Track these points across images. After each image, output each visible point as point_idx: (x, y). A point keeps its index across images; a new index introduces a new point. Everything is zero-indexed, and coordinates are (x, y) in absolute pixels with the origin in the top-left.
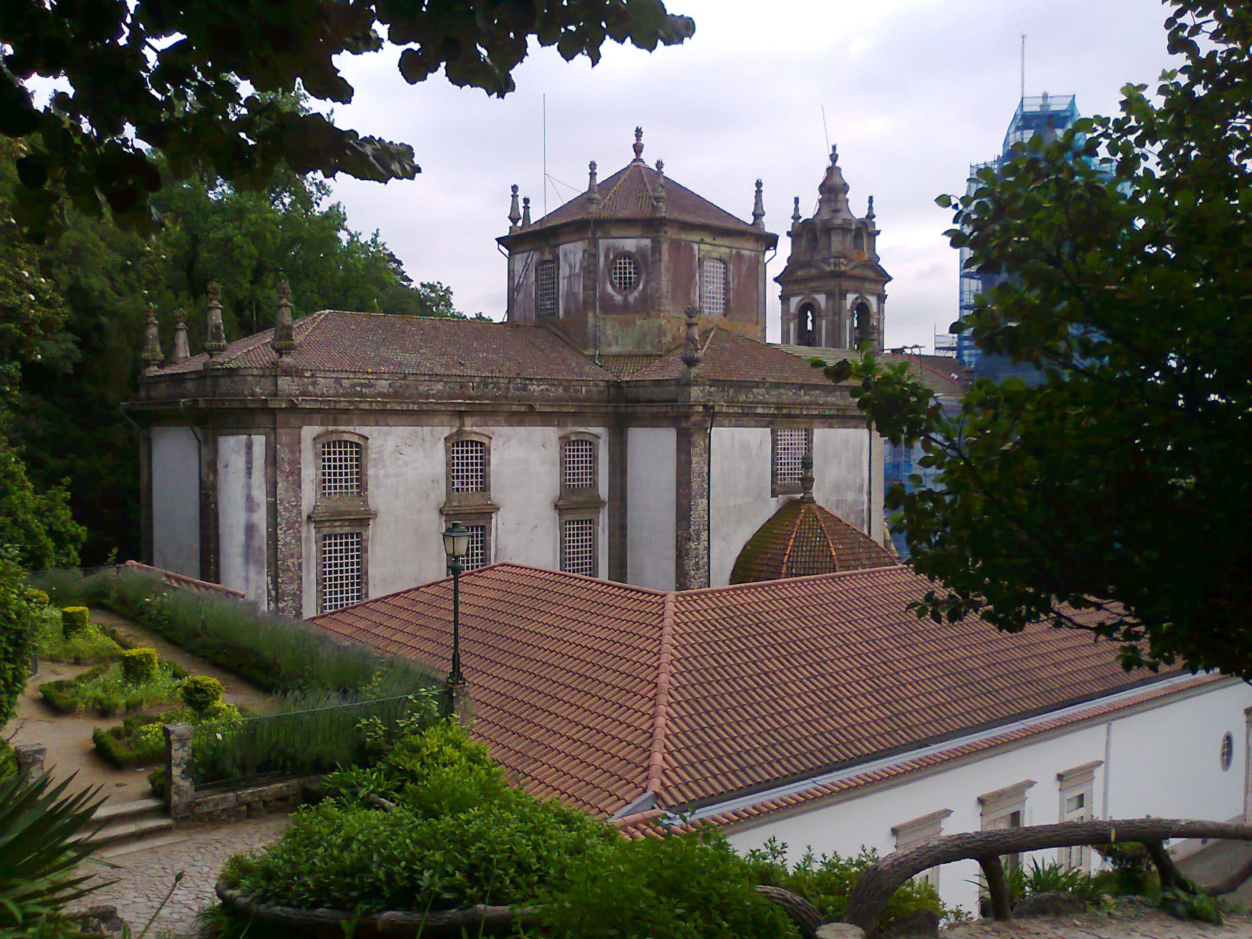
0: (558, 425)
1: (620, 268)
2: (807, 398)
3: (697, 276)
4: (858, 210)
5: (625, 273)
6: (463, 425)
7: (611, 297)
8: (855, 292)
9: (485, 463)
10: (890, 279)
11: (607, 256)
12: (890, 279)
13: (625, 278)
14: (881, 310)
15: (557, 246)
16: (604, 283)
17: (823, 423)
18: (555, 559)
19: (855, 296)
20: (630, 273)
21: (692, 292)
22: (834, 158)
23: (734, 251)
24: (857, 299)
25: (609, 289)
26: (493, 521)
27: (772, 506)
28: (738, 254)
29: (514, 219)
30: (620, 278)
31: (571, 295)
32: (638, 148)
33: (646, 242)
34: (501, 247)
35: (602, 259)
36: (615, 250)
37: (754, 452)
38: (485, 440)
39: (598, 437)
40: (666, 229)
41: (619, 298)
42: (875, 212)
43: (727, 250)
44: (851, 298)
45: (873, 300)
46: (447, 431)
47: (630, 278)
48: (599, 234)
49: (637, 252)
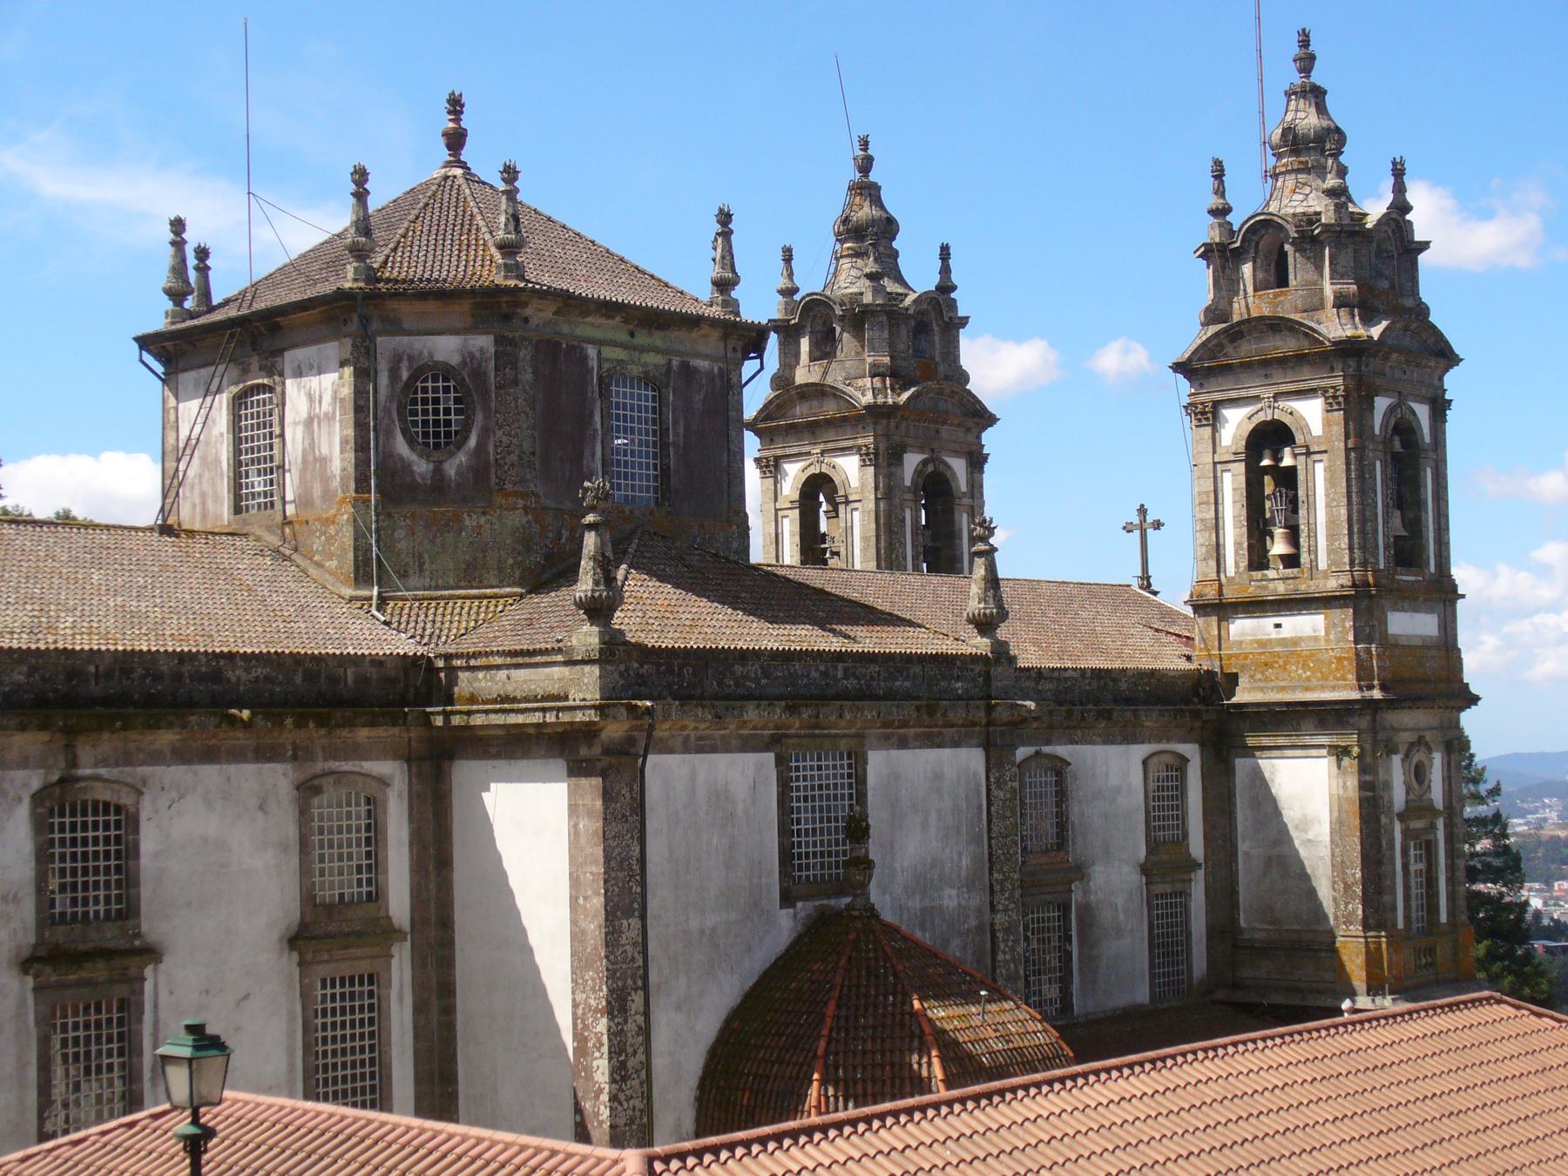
0: (295, 758)
1: (425, 401)
3: (597, 418)
4: (920, 276)
5: (436, 412)
6: (73, 763)
7: (406, 467)
8: (921, 450)
9: (126, 853)
11: (394, 373)
13: (436, 423)
14: (976, 488)
15: (280, 352)
18: (291, 1068)
19: (921, 457)
20: (447, 411)
21: (587, 453)
22: (866, 165)
23: (675, 362)
24: (925, 463)
25: (401, 447)
26: (148, 986)
27: (784, 926)
28: (685, 366)
29: (177, 296)
30: (426, 423)
31: (314, 462)
32: (455, 140)
33: (483, 342)
34: (148, 358)
35: (384, 380)
36: (410, 359)
37: (740, 808)
38: (126, 800)
39: (384, 782)
40: (528, 311)
41: (422, 467)
42: (955, 278)
43: (659, 360)
44: (912, 461)
45: (958, 466)
46: (35, 780)
47: (448, 423)
49: (464, 363)
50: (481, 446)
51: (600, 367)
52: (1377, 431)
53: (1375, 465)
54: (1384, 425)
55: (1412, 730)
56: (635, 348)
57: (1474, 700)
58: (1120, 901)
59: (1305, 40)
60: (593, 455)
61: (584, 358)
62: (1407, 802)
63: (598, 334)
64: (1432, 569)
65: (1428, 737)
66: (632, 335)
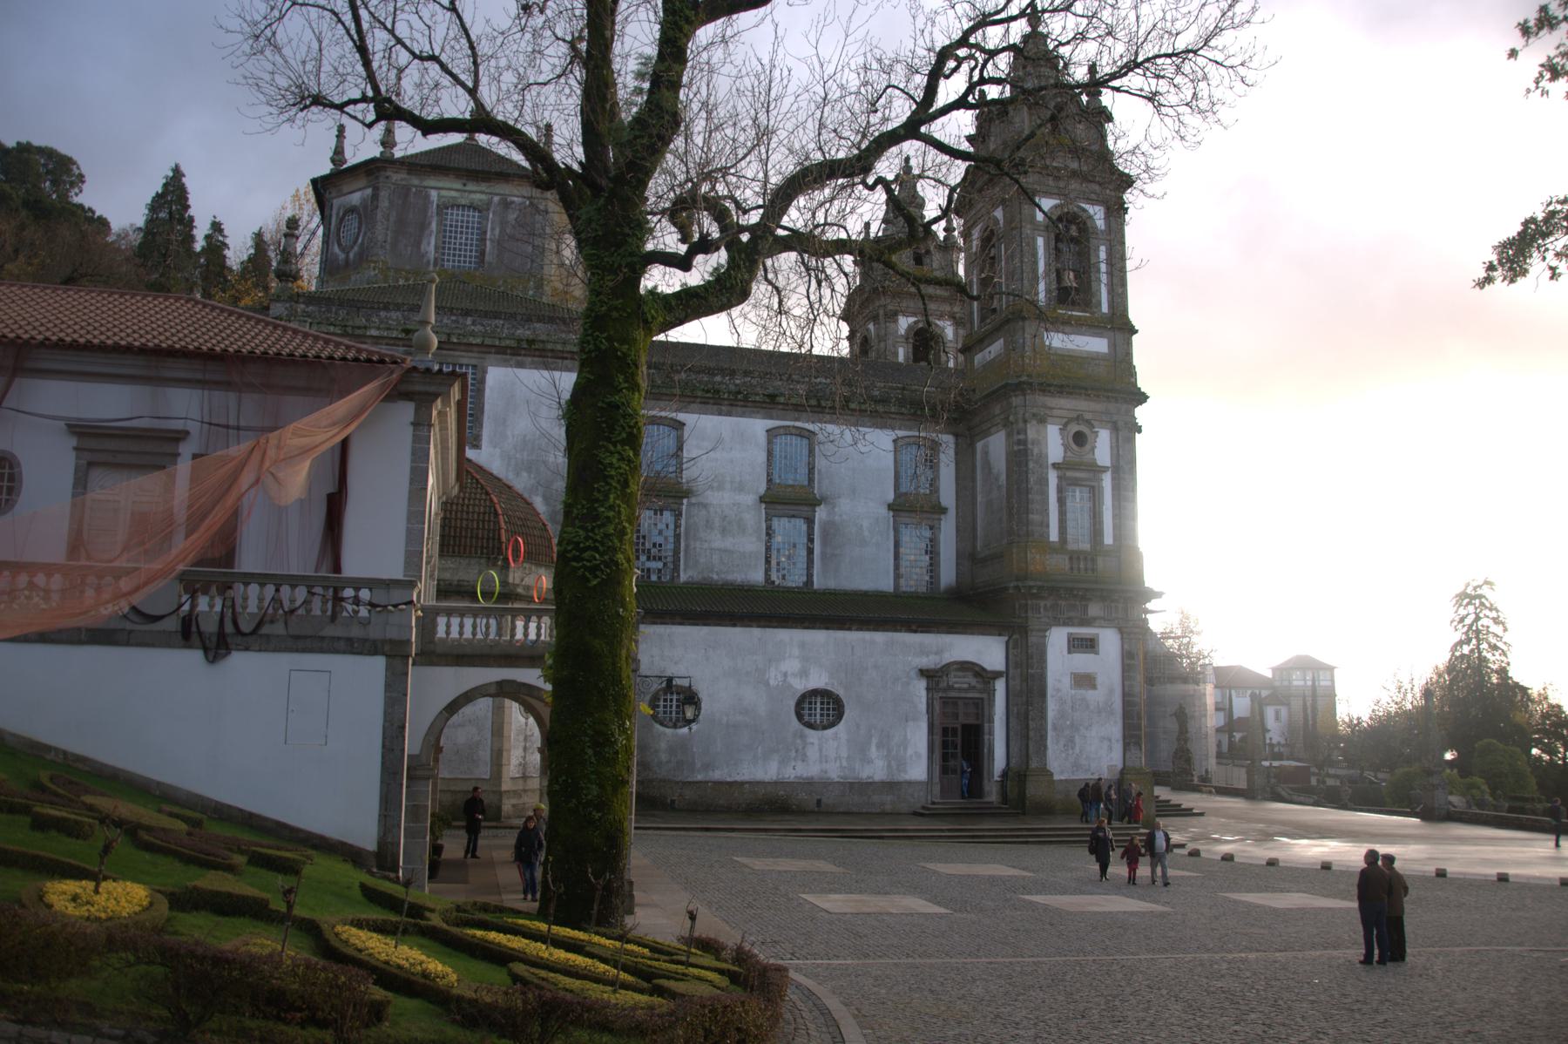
2: (478, 328)
3: (434, 226)
11: (338, 214)
16: (333, 245)
17: (505, 361)
21: (424, 242)
23: (496, 199)
33: (369, 191)
40: (389, 173)
43: (483, 197)
48: (334, 194)
50: (362, 243)
51: (438, 200)
53: (1034, 241)
56: (465, 191)
58: (866, 524)
60: (429, 244)
61: (427, 197)
62: (1064, 457)
63: (440, 184)
64: (1105, 308)
66: (465, 185)
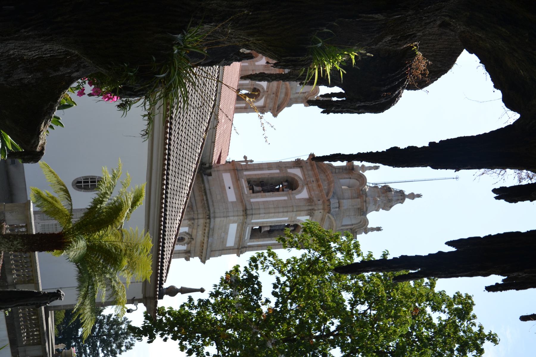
10: (275, 115)
12: (275, 115)
24: (263, 88)
45: (261, 103)
52: (298, 218)
54: (299, 221)
55: (196, 235)
57: (204, 262)
59: (419, 196)
64: (249, 244)
65: (193, 242)
